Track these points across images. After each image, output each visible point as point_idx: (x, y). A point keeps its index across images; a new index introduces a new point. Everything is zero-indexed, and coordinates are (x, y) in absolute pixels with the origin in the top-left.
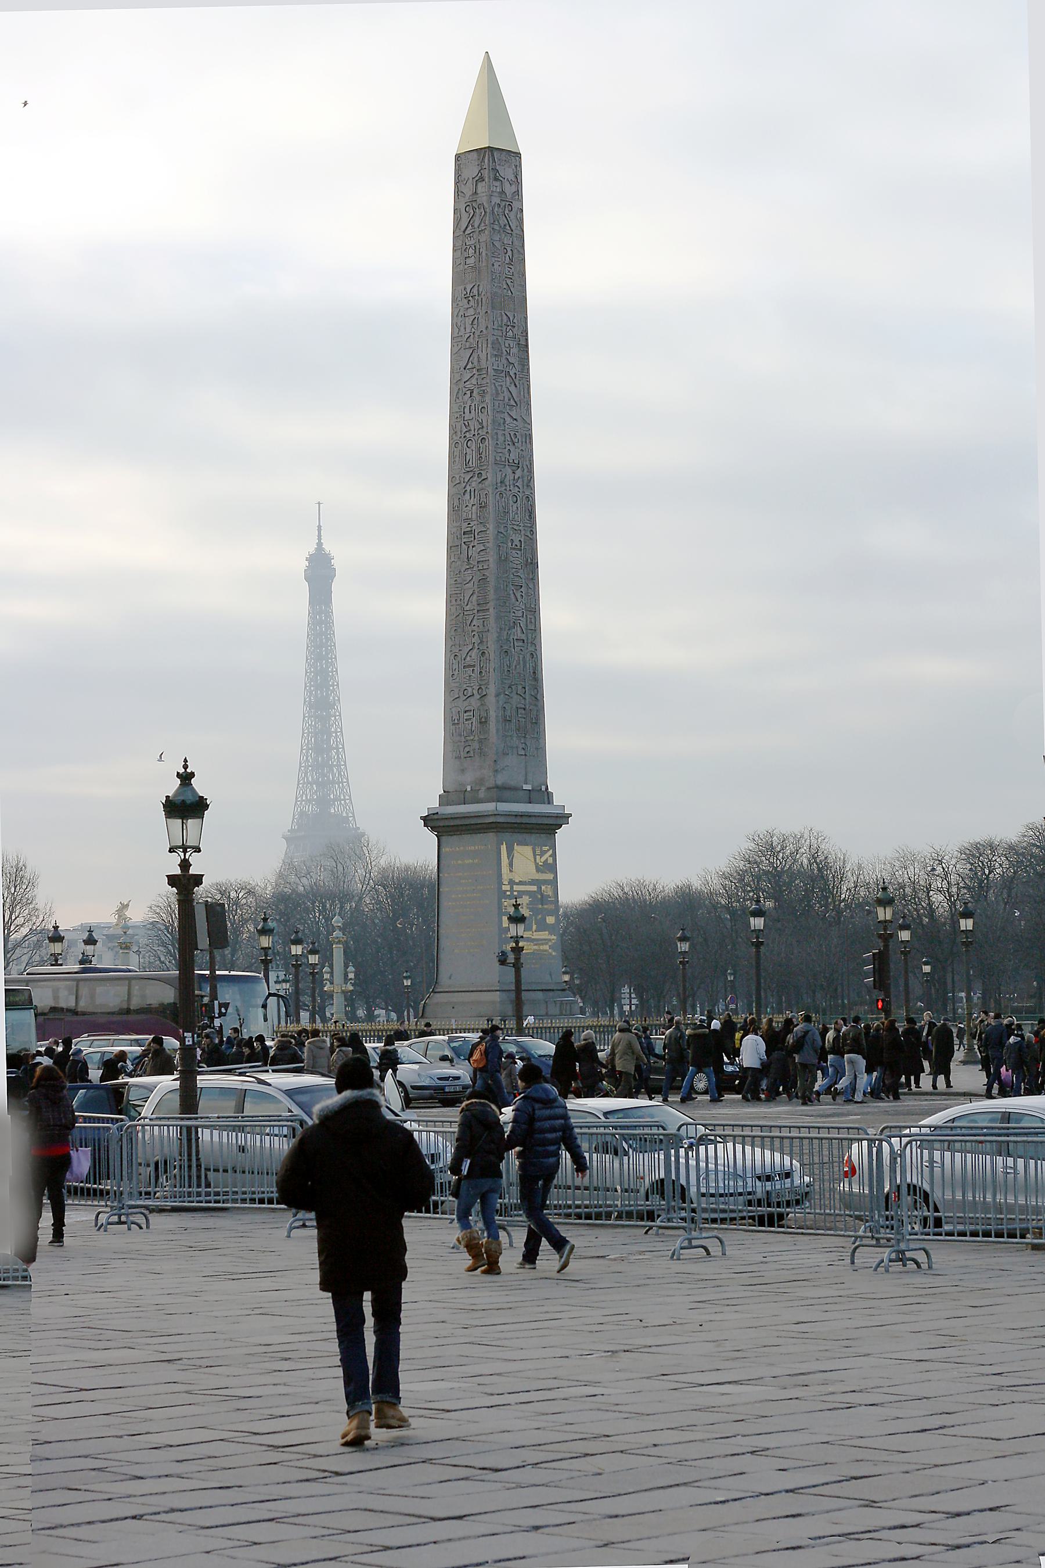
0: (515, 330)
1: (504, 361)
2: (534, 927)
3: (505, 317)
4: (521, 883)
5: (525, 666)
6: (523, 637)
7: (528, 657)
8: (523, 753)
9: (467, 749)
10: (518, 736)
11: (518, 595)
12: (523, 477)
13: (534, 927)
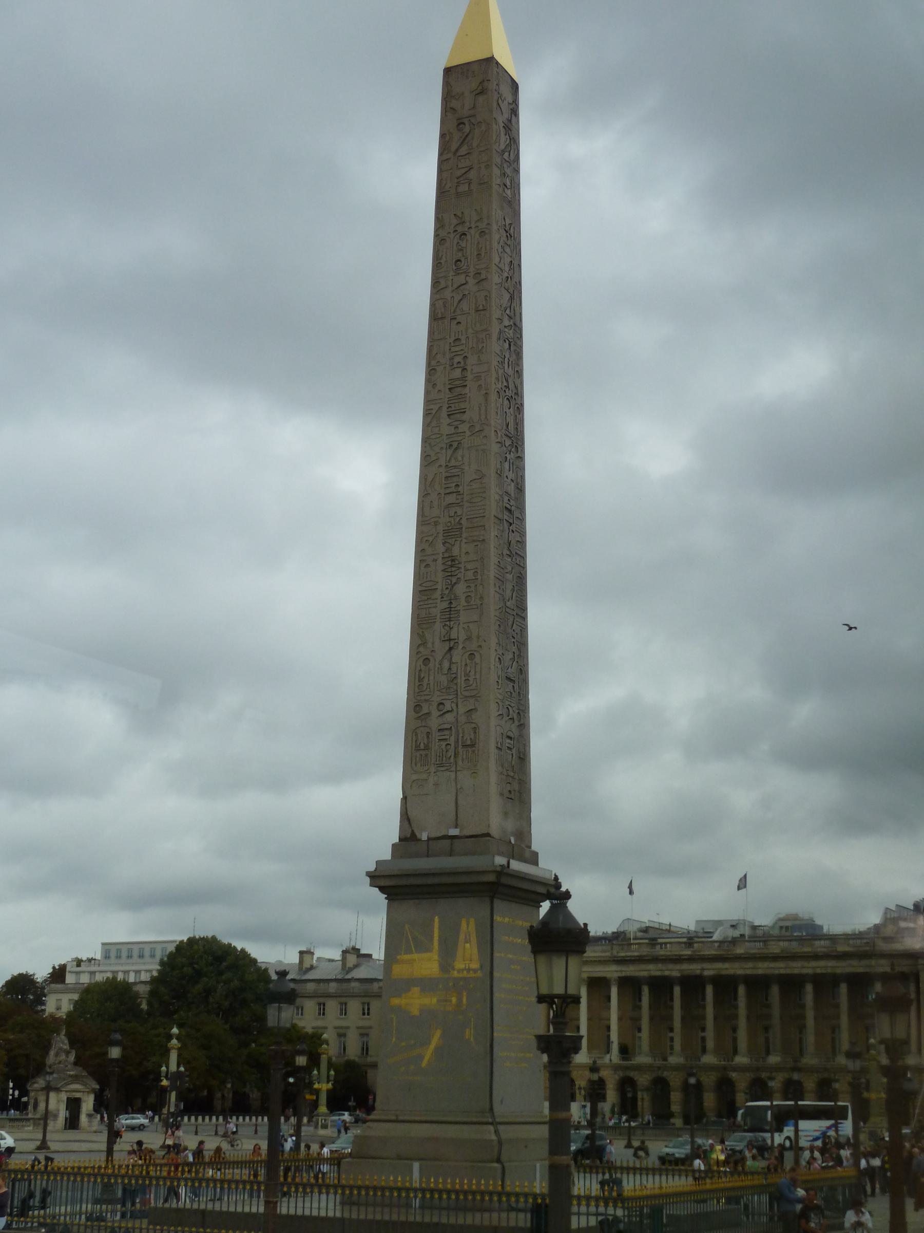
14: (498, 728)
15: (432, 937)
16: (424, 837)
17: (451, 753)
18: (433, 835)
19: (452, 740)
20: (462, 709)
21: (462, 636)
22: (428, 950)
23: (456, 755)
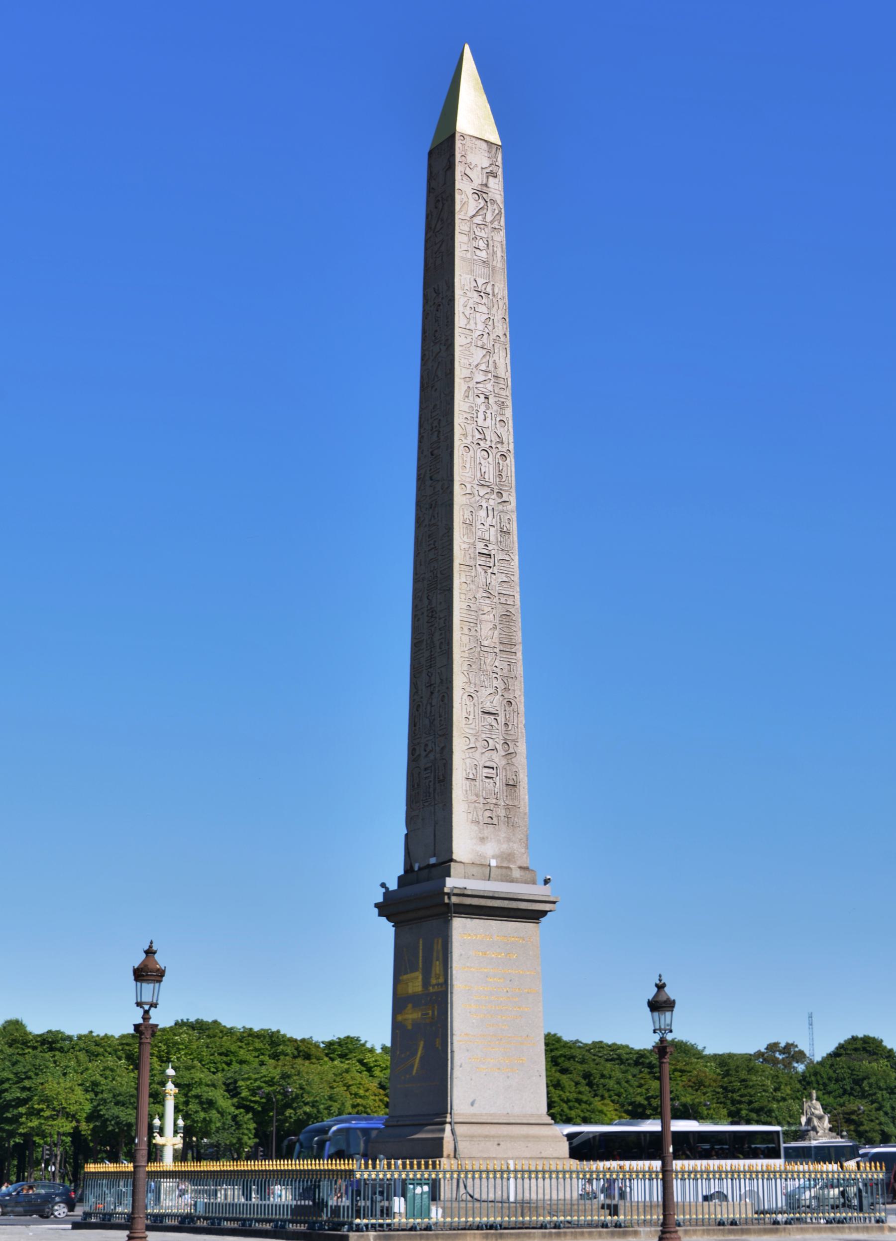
9: (488, 814)
14: (468, 761)
15: (418, 957)
16: (416, 869)
17: (431, 790)
18: (422, 866)
19: (432, 779)
20: (438, 749)
21: (438, 681)
22: (417, 970)
23: (435, 790)
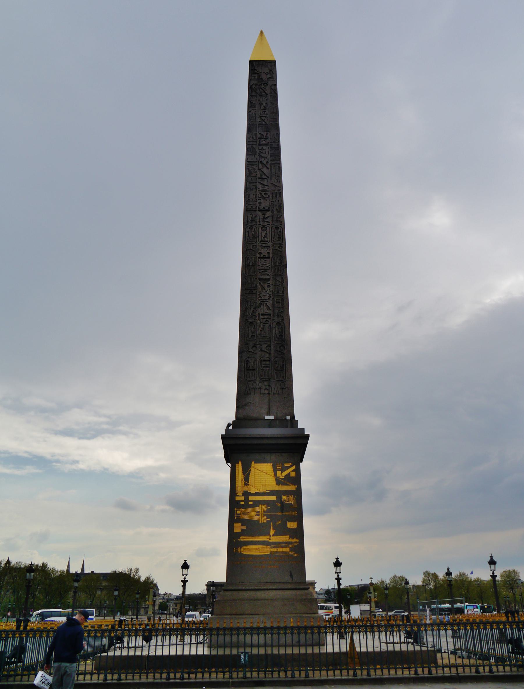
0: (267, 141)
1: (257, 156)
2: (272, 532)
3: (259, 136)
4: (257, 494)
5: (271, 330)
6: (269, 312)
7: (274, 325)
8: (266, 392)
10: (262, 381)
11: (266, 286)
12: (272, 216)
13: (272, 532)
